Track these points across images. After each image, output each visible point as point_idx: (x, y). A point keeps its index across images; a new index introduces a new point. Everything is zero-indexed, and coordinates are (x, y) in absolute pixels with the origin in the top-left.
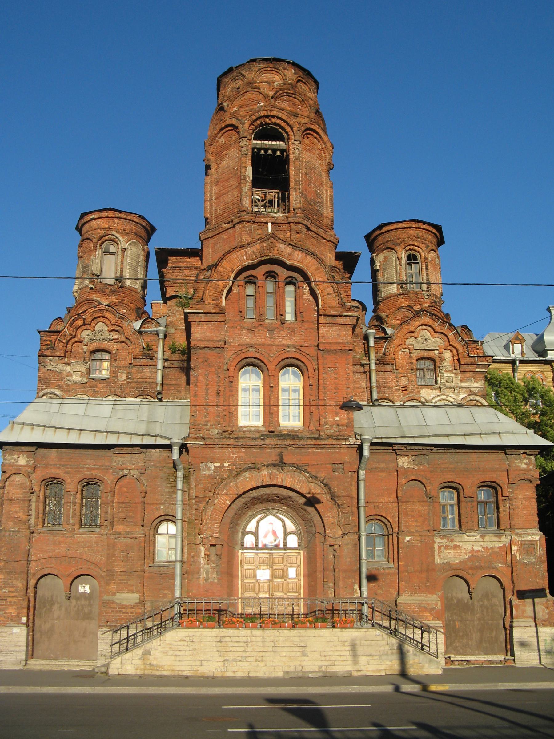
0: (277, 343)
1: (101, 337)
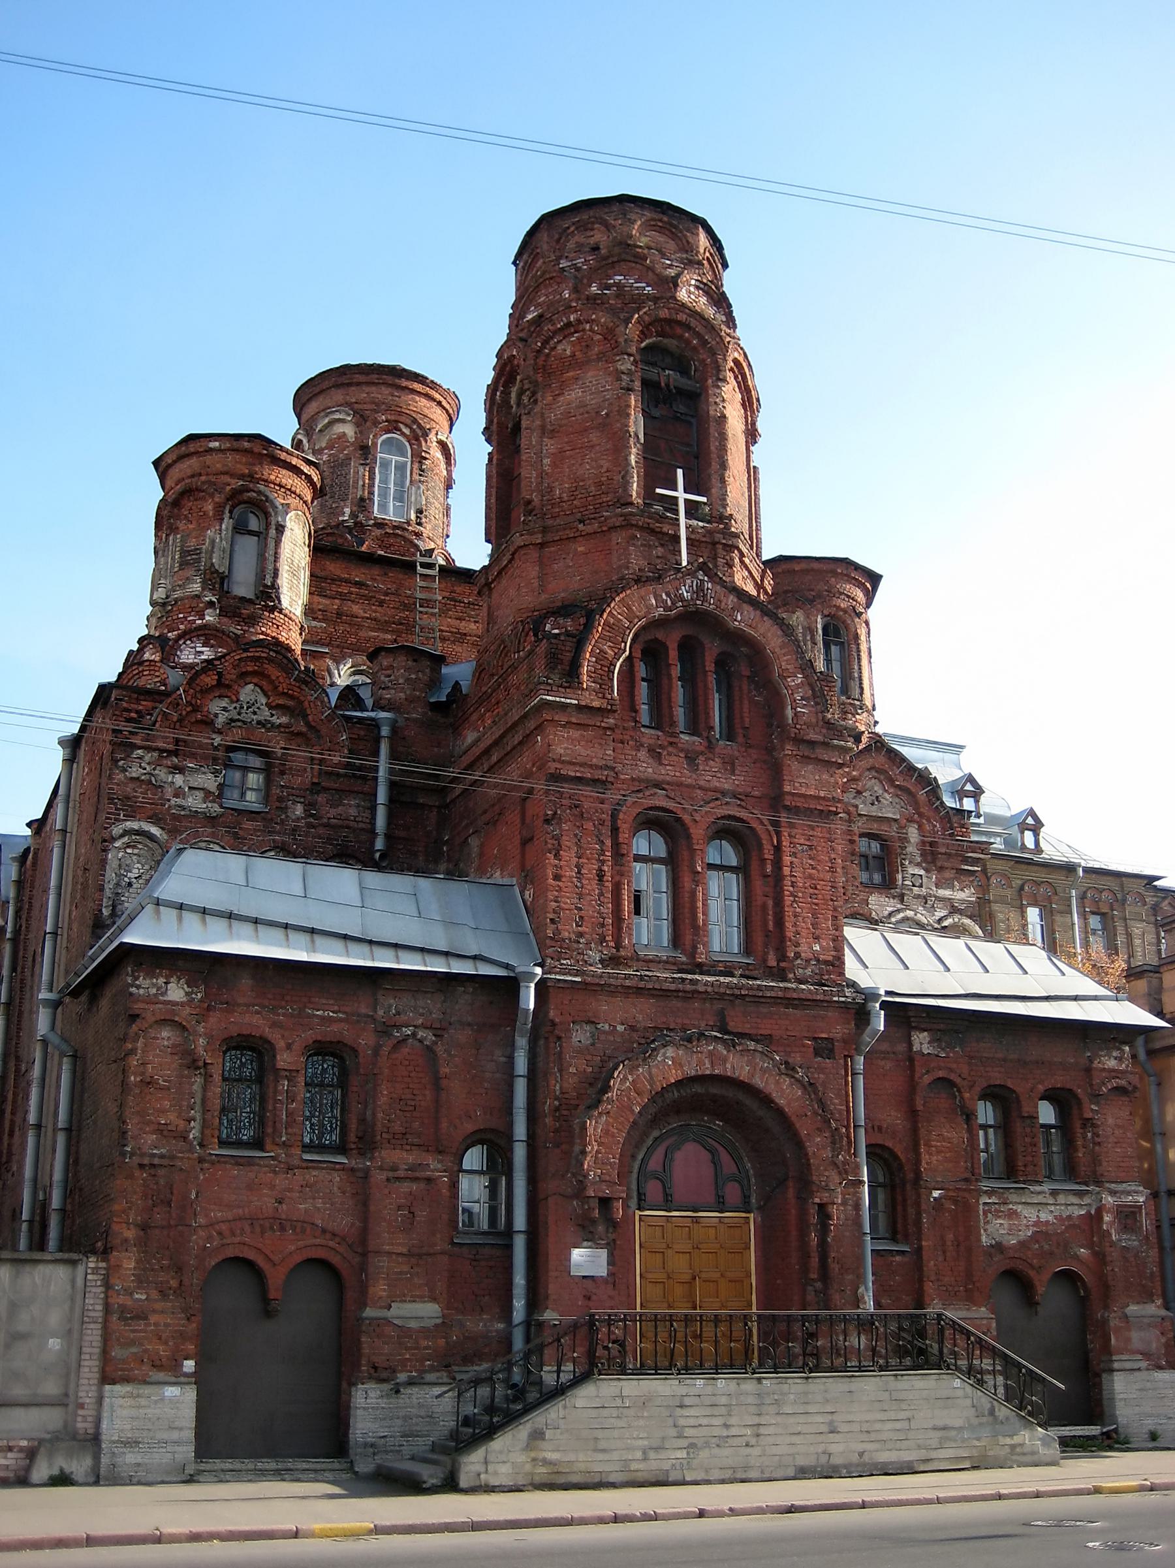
0: (702, 783)
1: (255, 717)
